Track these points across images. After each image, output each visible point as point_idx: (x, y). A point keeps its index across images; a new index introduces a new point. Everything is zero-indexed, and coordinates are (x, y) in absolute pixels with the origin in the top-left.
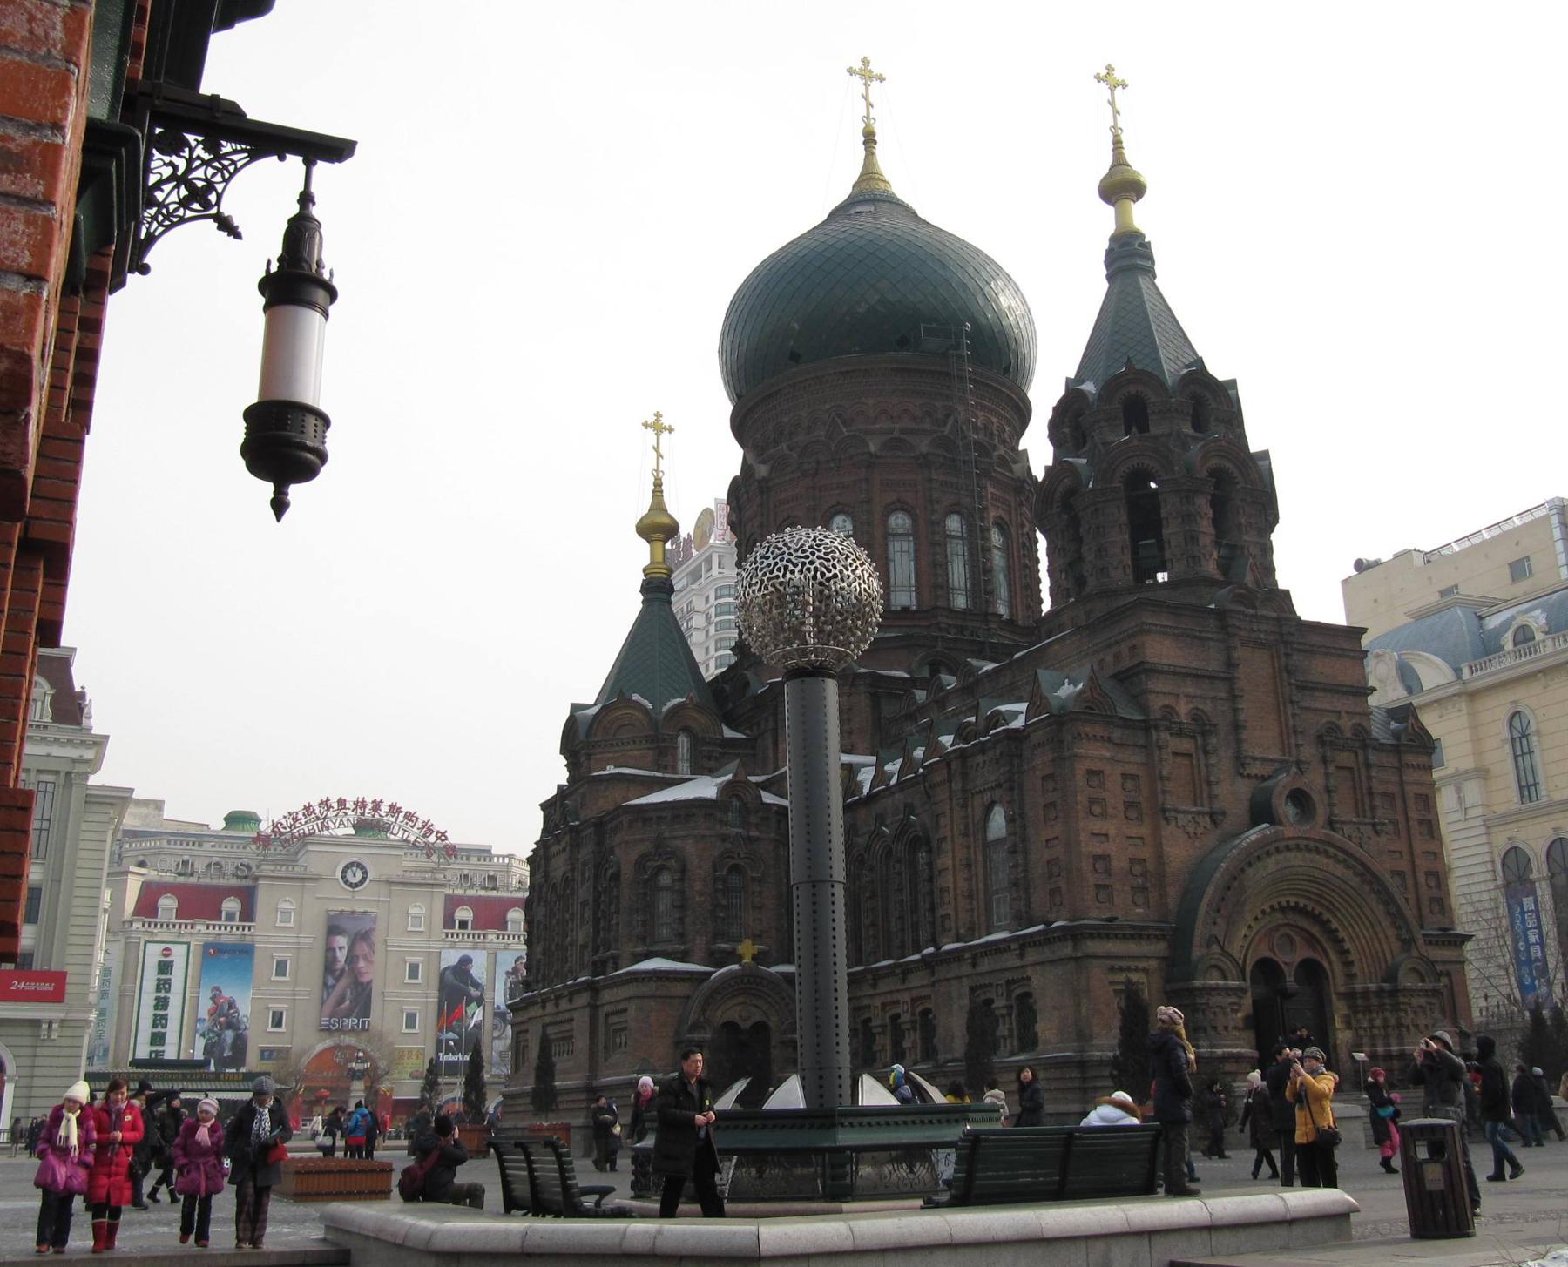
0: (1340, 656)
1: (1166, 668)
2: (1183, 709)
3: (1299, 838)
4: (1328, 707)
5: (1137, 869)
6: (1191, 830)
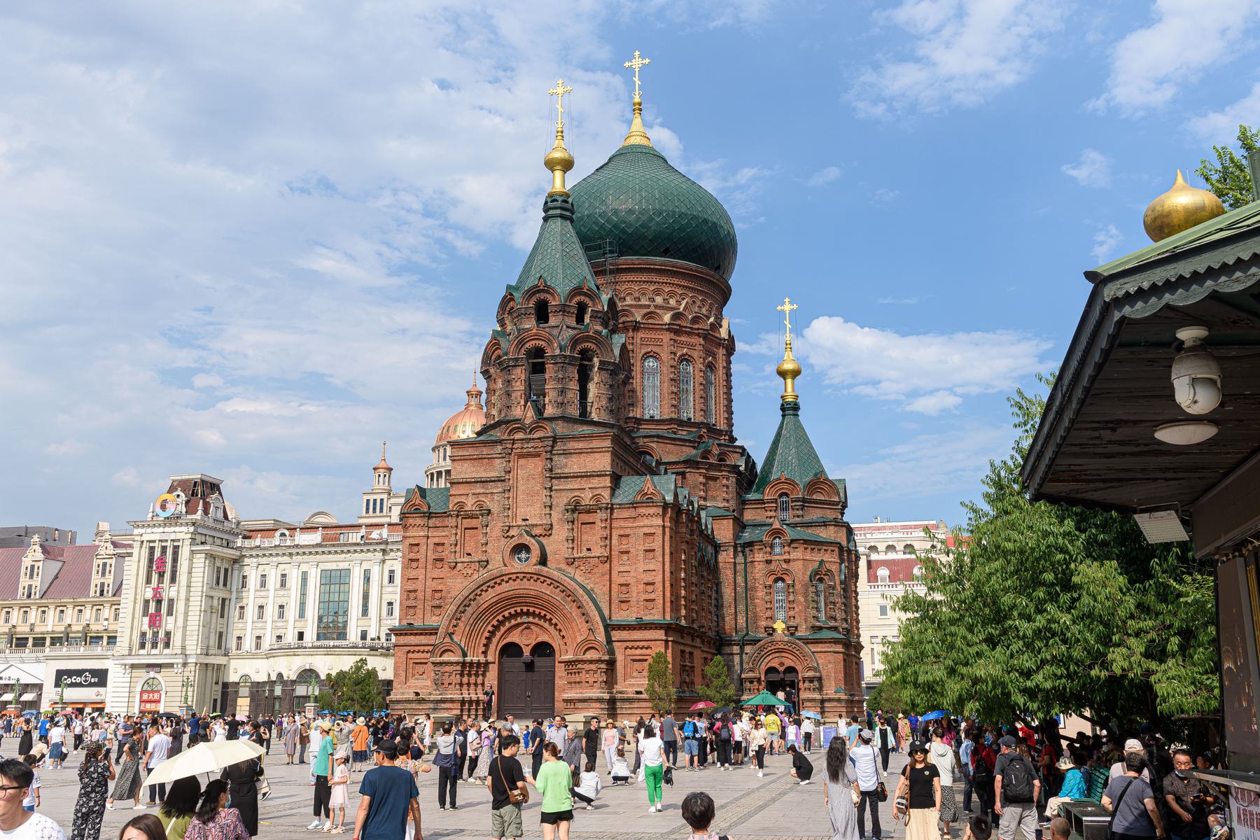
0: (591, 452)
1: (461, 480)
3: (518, 573)
4: (576, 487)
5: (437, 595)
6: (465, 573)
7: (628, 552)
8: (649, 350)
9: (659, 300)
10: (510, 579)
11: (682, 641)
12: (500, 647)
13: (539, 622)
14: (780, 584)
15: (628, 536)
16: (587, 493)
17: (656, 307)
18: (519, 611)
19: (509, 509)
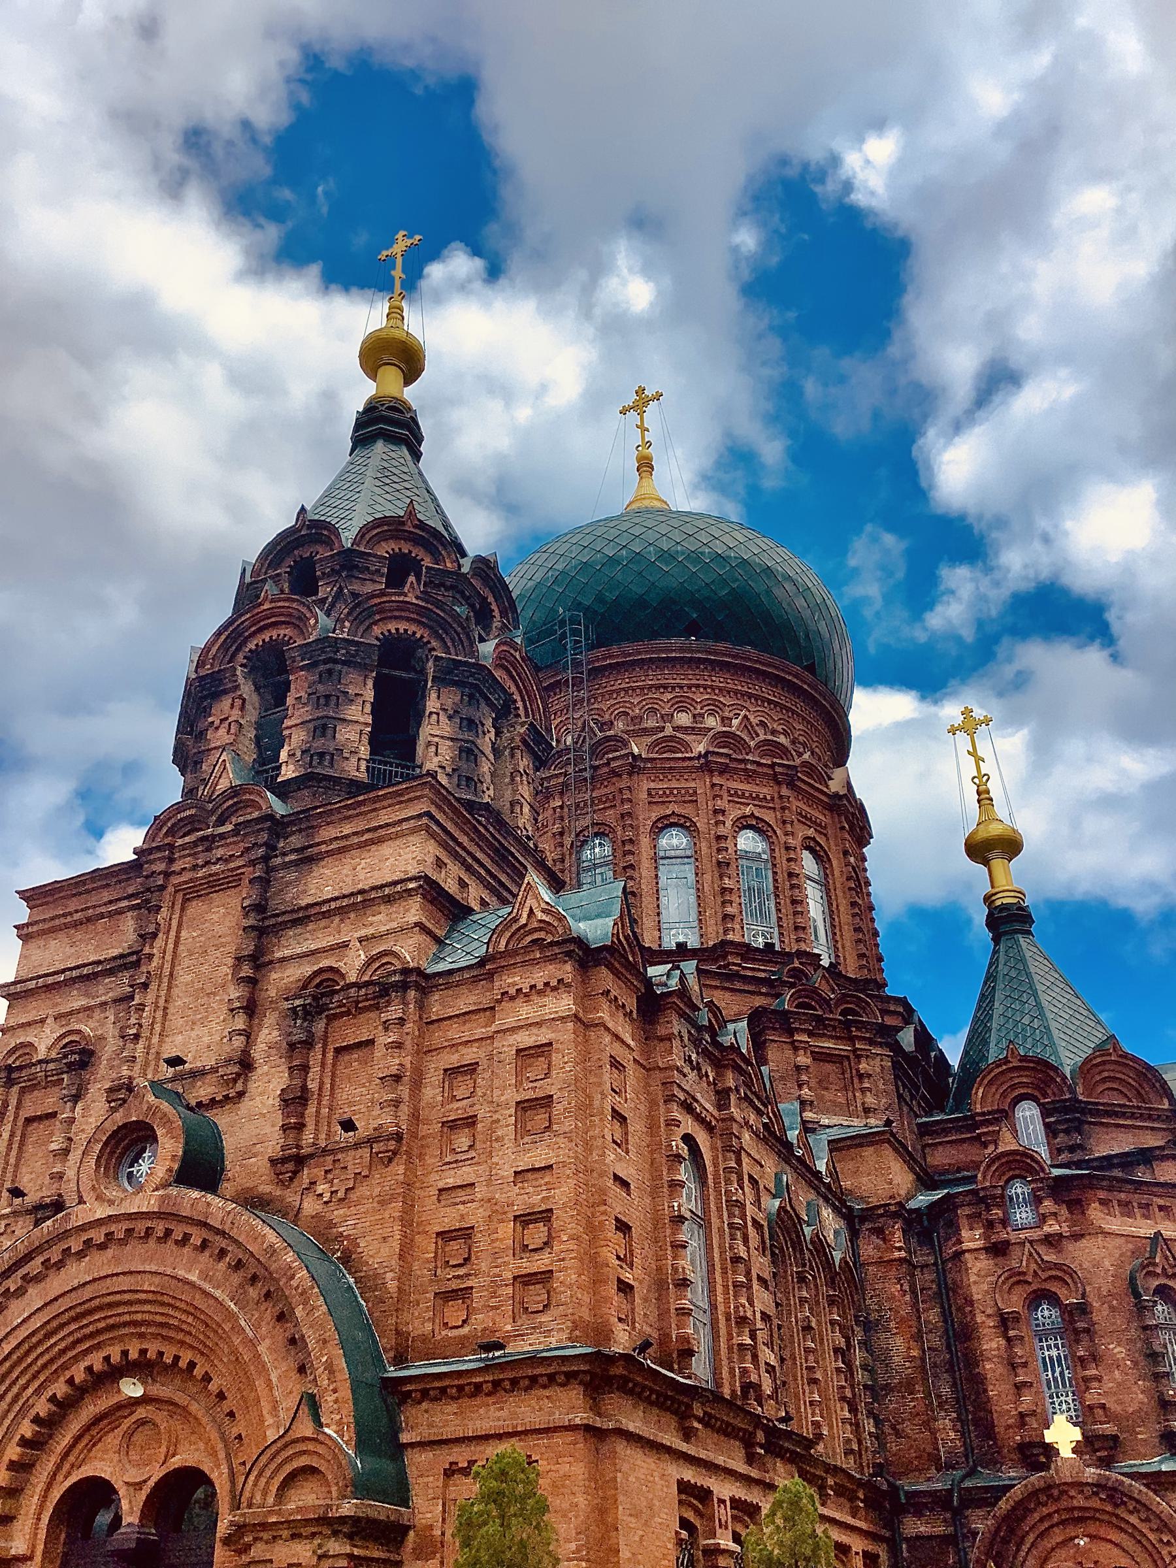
0: (373, 842)
2: (44, 1041)
7: (470, 1122)
8: (669, 812)
9: (684, 719)
10: (88, 1242)
11: (684, 1447)
12: (56, 1494)
13: (180, 1398)
14: (1046, 1314)
15: (471, 1069)
16: (351, 953)
17: (677, 728)
18: (116, 1358)
19: (137, 1037)
